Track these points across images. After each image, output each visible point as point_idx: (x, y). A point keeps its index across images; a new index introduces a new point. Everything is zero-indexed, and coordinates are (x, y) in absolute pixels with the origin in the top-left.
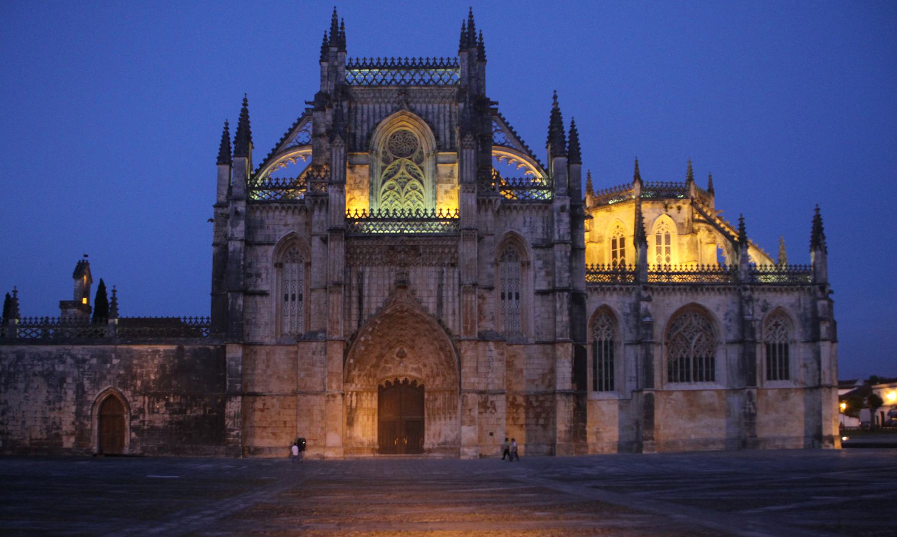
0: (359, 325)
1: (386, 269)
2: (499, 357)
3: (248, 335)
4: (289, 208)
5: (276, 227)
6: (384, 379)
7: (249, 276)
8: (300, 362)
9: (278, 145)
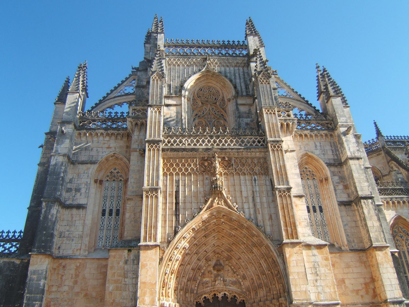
2: (326, 262)
3: (59, 248)
5: (99, 149)
7: (69, 190)
9: (108, 94)
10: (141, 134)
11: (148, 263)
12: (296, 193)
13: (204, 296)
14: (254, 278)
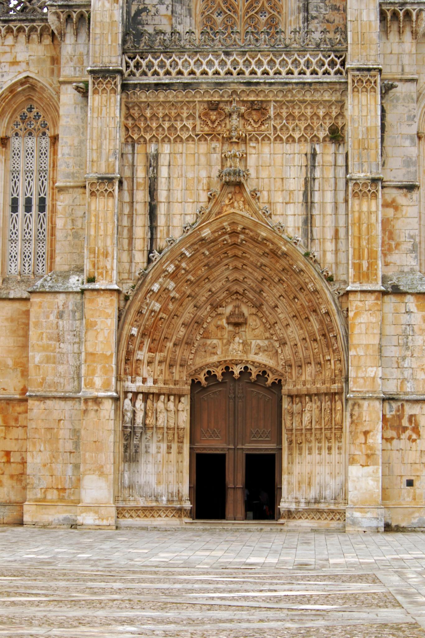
0: (149, 261)
1: (203, 147)
4: (20, 29)
6: (202, 369)
8: (33, 333)
10: (79, 41)
11: (98, 321)
12: (402, 179)
13: (207, 370)
14: (299, 344)
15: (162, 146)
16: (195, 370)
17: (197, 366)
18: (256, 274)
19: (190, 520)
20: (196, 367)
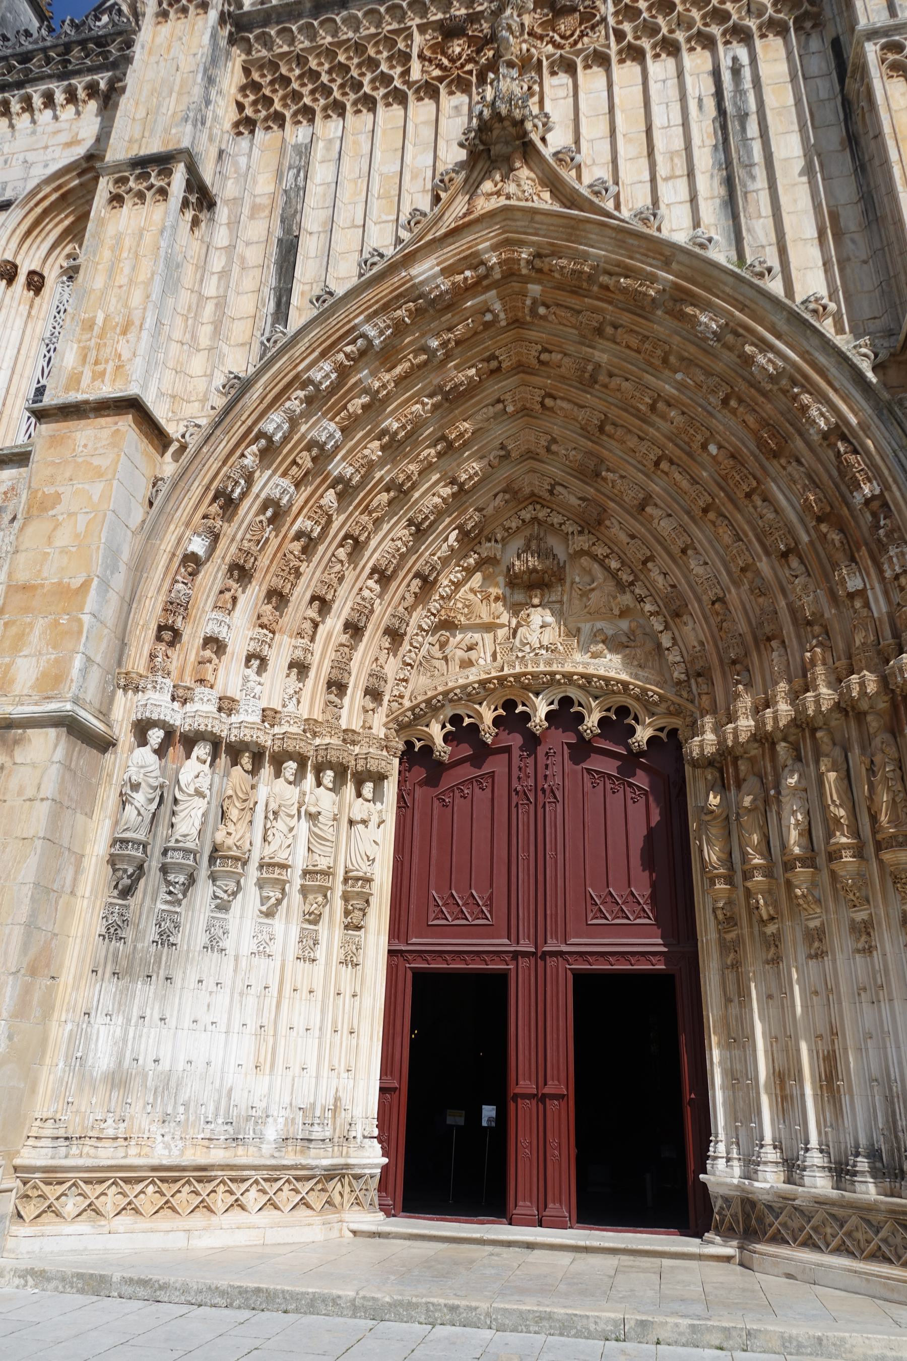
6: (432, 707)
13: (449, 712)
15: (324, 126)
16: (412, 709)
17: (420, 699)
18: (581, 415)
19: (373, 1220)
20: (415, 702)
